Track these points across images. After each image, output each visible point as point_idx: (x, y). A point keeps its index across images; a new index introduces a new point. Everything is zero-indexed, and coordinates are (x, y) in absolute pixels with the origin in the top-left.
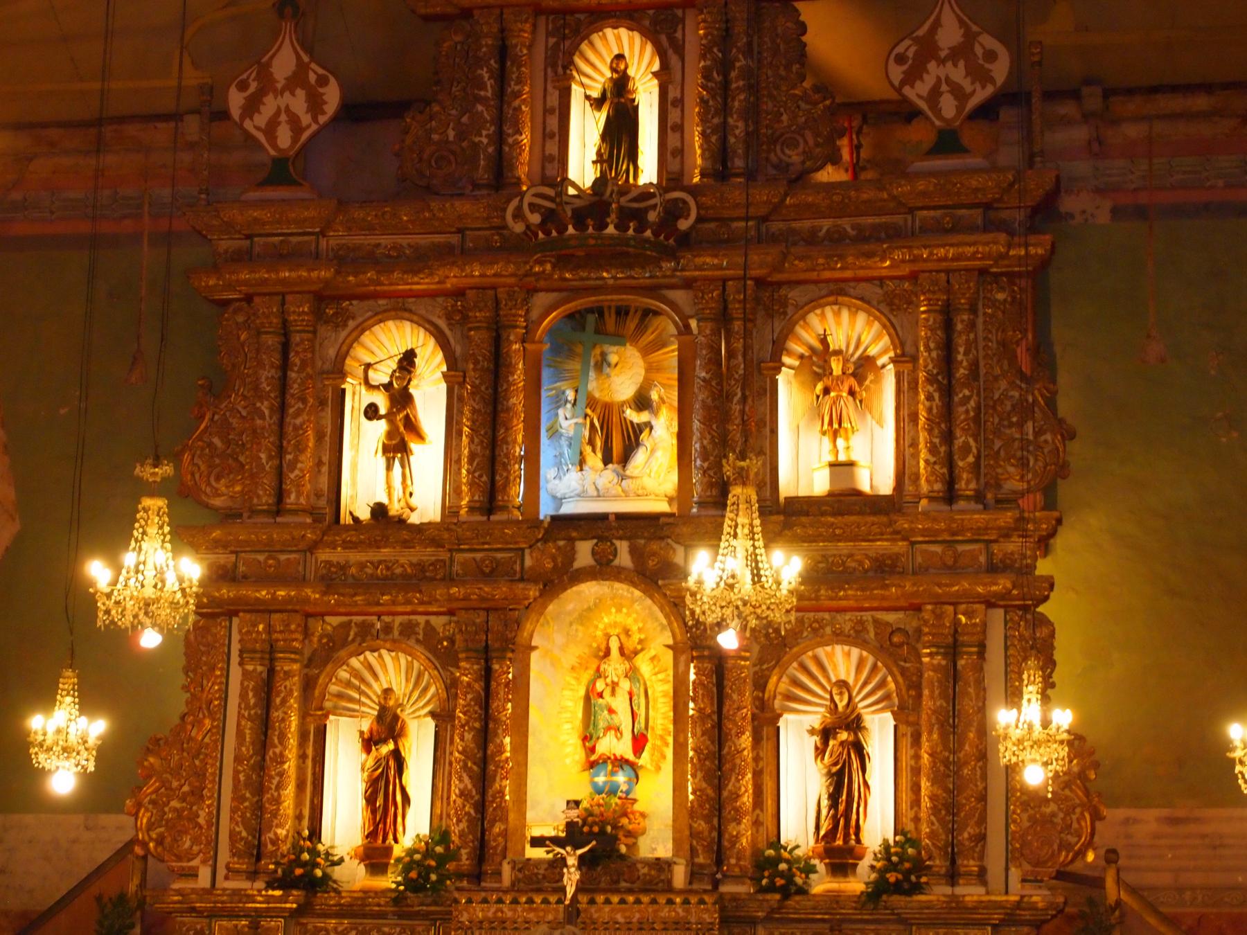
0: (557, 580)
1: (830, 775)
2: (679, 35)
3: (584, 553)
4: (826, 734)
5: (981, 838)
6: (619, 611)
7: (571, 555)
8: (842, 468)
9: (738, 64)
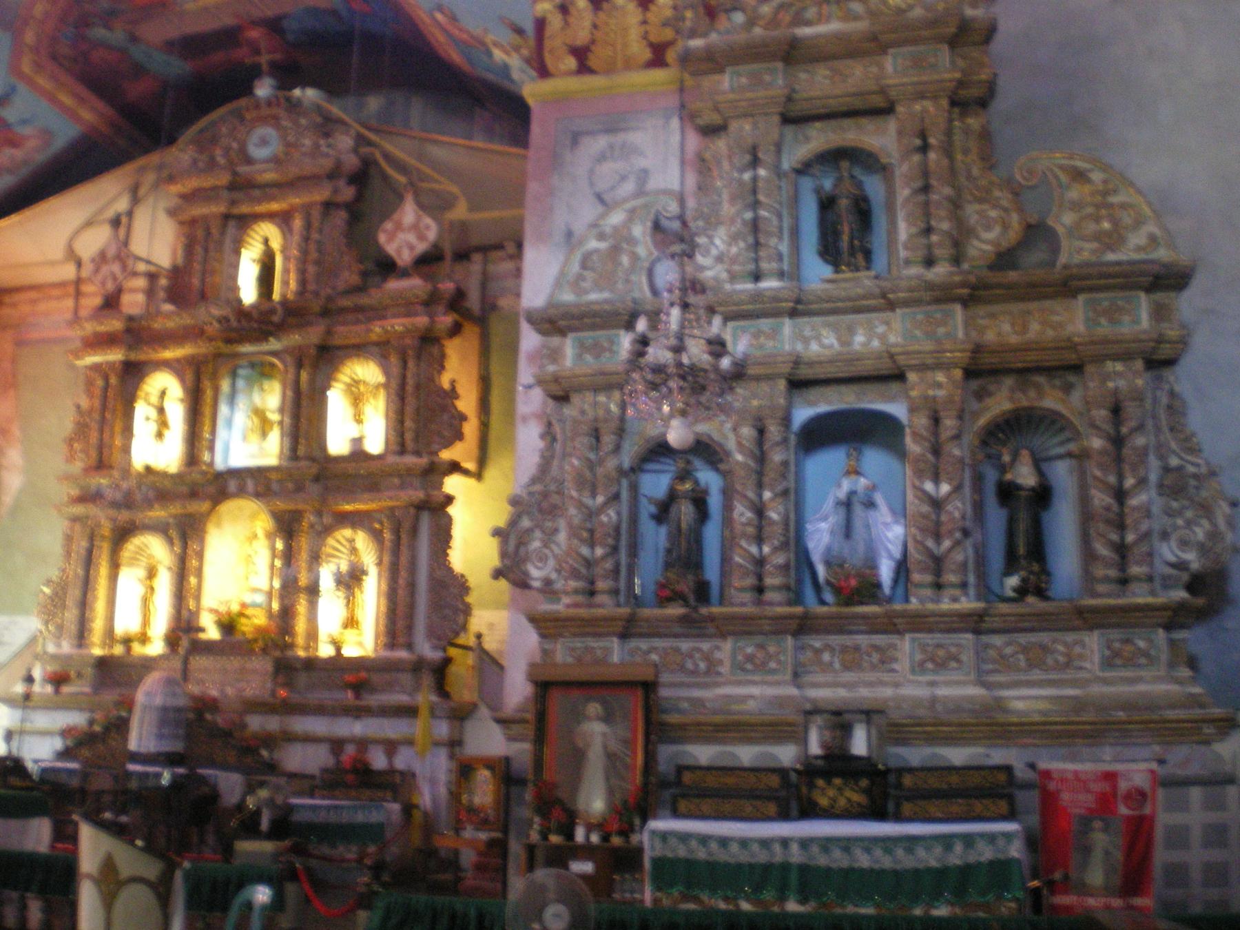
3: (232, 486)
8: (358, 441)
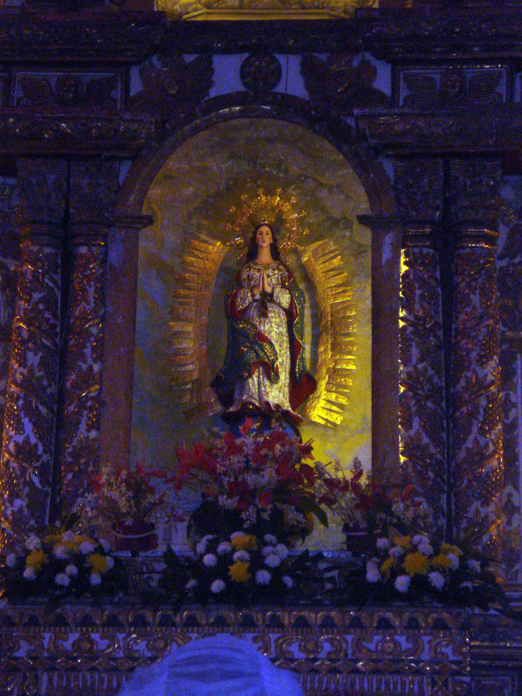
0: (184, 107)
3: (227, 74)
7: (205, 74)
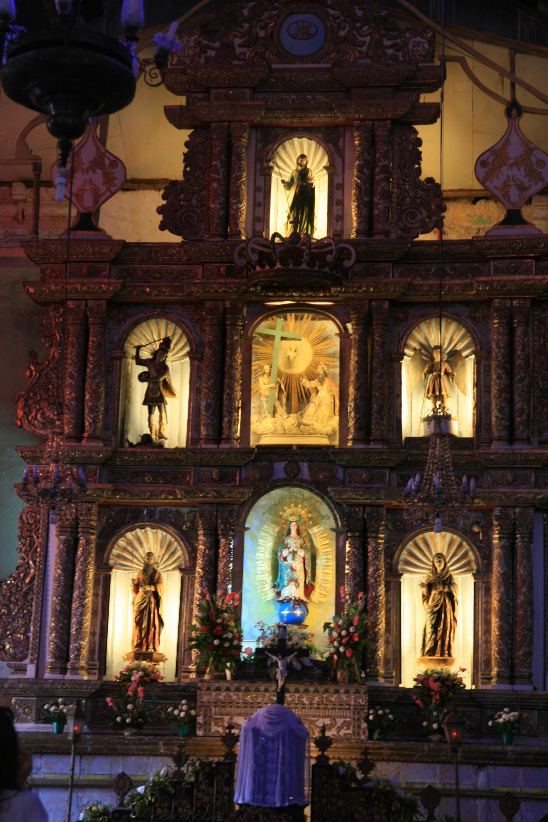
1: (433, 613)
2: (341, 144)
4: (430, 586)
5: (529, 654)
6: (296, 506)
9: (380, 164)
